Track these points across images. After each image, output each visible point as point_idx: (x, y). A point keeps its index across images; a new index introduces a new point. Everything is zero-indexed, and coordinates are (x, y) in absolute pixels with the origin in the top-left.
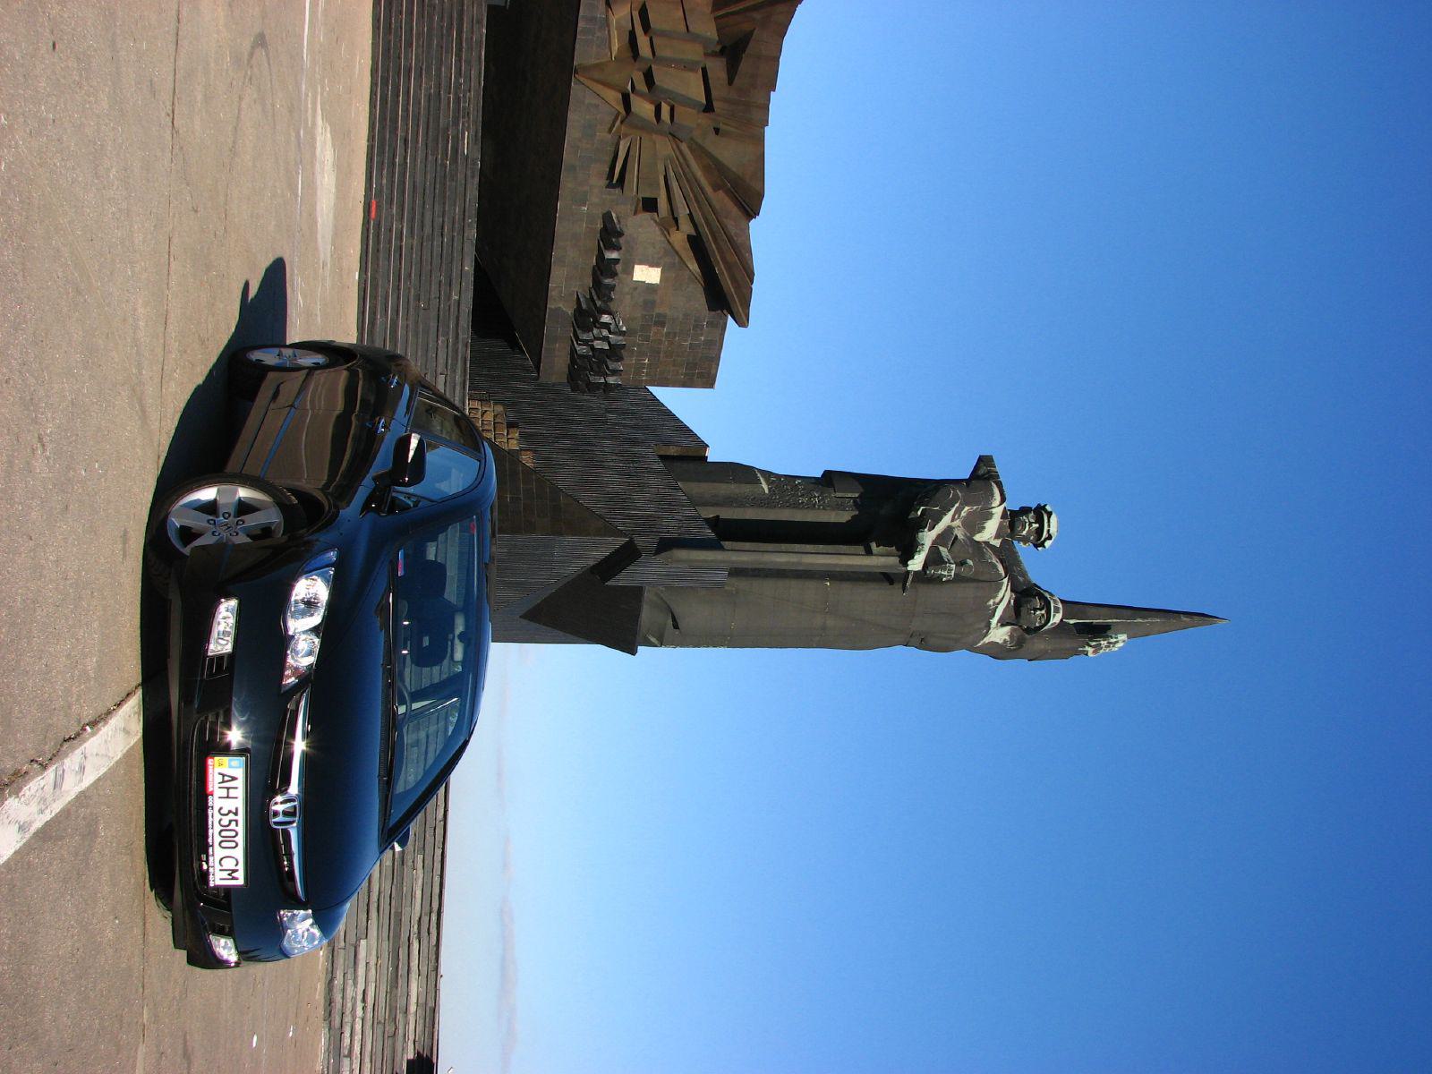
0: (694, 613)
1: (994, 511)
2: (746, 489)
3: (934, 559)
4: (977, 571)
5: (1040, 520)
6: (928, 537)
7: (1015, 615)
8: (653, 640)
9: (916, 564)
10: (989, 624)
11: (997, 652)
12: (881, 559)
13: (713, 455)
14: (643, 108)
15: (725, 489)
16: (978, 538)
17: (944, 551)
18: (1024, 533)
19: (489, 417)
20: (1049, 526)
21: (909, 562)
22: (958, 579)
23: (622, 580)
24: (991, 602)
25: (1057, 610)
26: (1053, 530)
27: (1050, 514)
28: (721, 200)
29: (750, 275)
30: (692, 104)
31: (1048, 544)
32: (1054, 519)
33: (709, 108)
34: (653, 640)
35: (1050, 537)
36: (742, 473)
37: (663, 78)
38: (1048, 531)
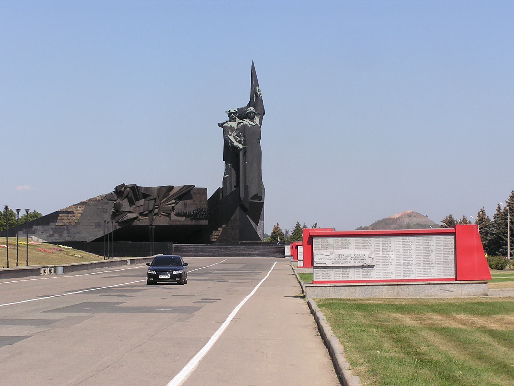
0: (253, 192)
2: (228, 180)
3: (240, 142)
4: (243, 131)
5: (232, 113)
6: (236, 144)
7: (252, 119)
9: (241, 146)
11: (261, 121)
12: (241, 154)
14: (156, 211)
15: (228, 185)
16: (236, 128)
17: (239, 139)
19: (216, 234)
22: (244, 136)
23: (247, 206)
25: (251, 110)
28: (172, 193)
30: (155, 202)
33: (155, 199)
36: (225, 180)
37: (151, 208)
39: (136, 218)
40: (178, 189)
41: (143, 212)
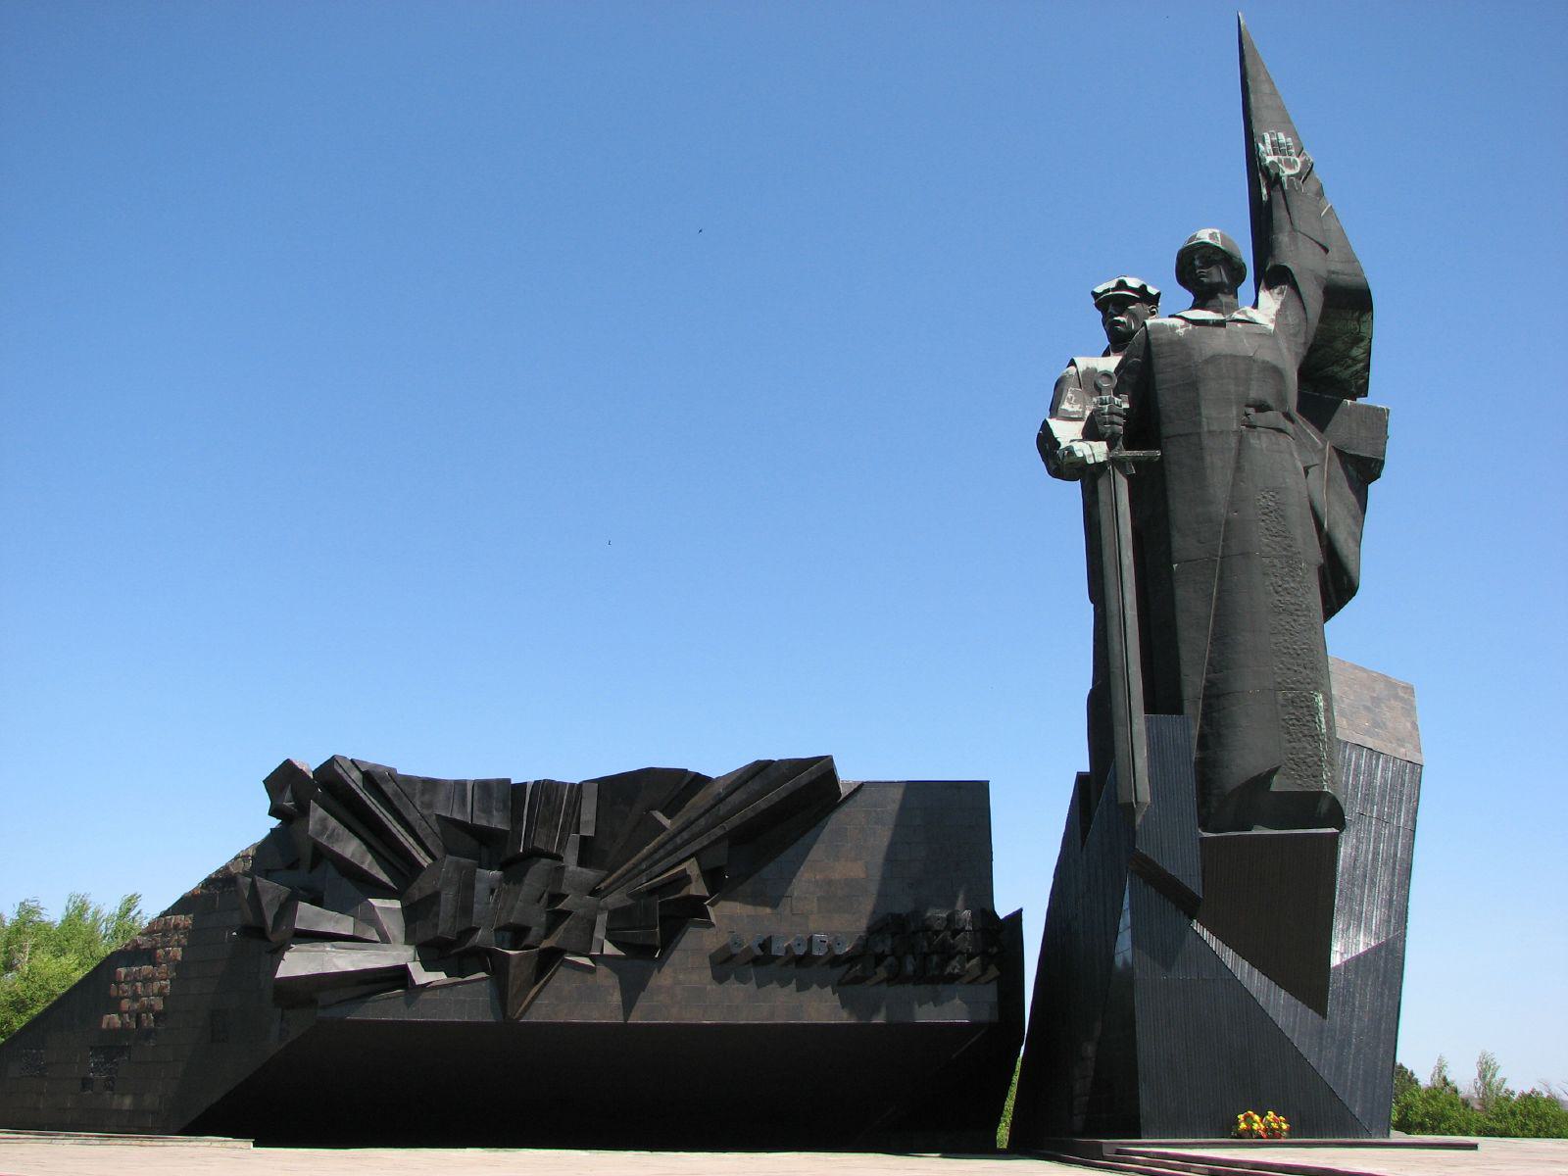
1: (1081, 370)
8: (1324, 807)
10: (1220, 324)
13: (1086, 768)
18: (1122, 319)
20: (1108, 290)
21: (1090, 461)
24: (1181, 331)
26: (1113, 284)
27: (1095, 295)
29: (760, 769)
31: (1133, 282)
32: (1099, 290)
34: (1324, 807)
35: (1122, 285)
38: (1114, 290)
39: (399, 976)
40: (719, 789)
41: (450, 944)
